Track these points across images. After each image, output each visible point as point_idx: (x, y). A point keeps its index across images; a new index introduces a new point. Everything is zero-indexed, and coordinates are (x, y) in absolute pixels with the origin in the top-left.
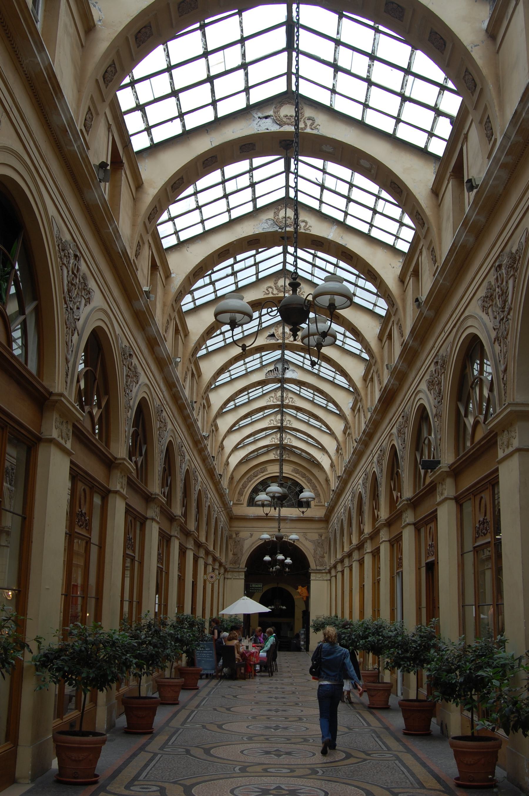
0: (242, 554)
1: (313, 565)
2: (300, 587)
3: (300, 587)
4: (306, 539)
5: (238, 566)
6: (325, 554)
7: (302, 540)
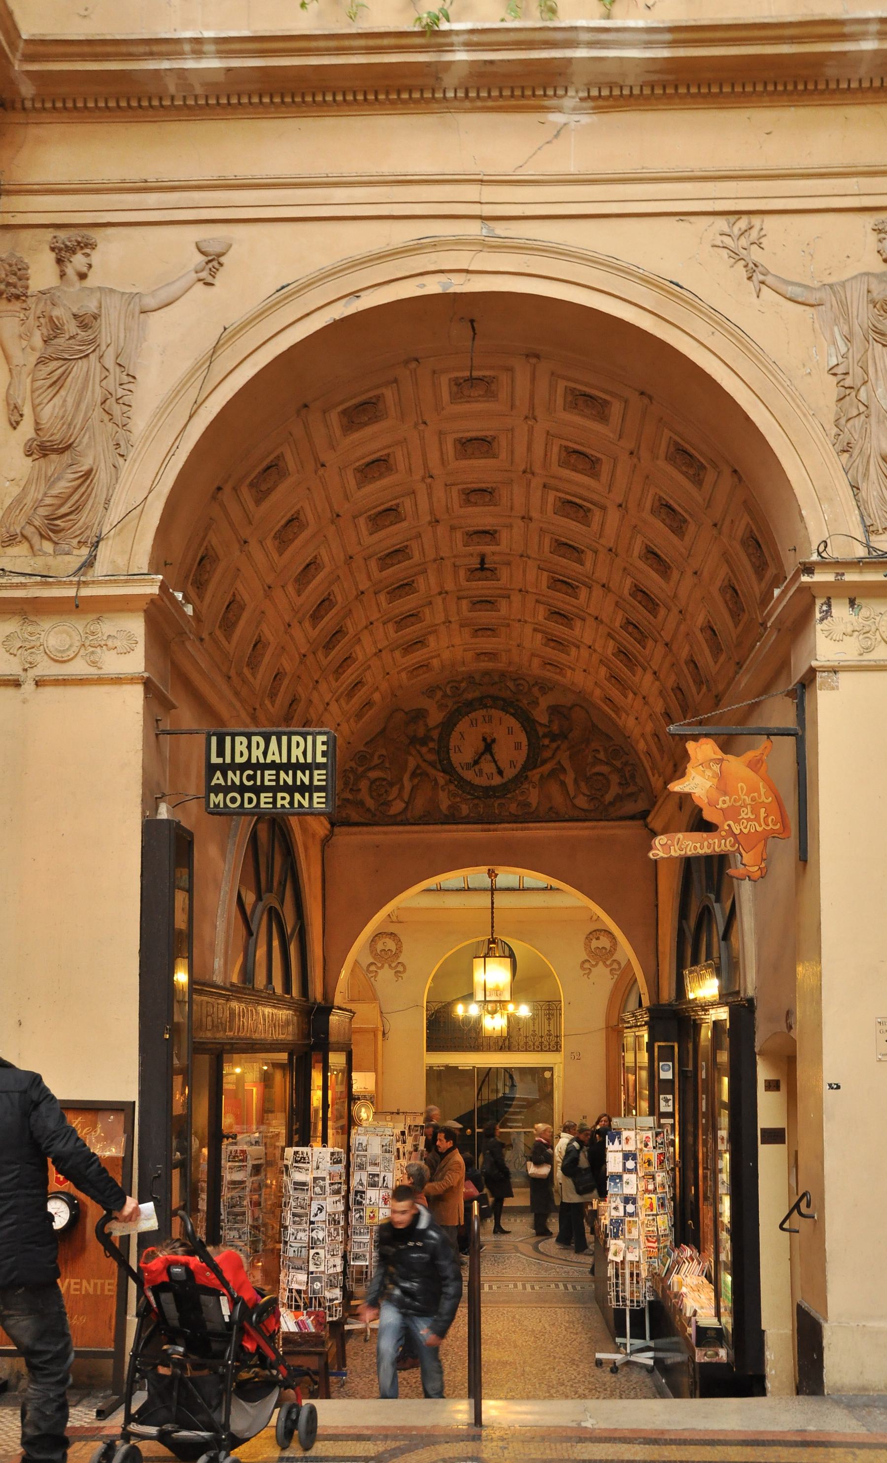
2: (702, 751)
3: (702, 751)
4: (752, 269)
7: (715, 281)
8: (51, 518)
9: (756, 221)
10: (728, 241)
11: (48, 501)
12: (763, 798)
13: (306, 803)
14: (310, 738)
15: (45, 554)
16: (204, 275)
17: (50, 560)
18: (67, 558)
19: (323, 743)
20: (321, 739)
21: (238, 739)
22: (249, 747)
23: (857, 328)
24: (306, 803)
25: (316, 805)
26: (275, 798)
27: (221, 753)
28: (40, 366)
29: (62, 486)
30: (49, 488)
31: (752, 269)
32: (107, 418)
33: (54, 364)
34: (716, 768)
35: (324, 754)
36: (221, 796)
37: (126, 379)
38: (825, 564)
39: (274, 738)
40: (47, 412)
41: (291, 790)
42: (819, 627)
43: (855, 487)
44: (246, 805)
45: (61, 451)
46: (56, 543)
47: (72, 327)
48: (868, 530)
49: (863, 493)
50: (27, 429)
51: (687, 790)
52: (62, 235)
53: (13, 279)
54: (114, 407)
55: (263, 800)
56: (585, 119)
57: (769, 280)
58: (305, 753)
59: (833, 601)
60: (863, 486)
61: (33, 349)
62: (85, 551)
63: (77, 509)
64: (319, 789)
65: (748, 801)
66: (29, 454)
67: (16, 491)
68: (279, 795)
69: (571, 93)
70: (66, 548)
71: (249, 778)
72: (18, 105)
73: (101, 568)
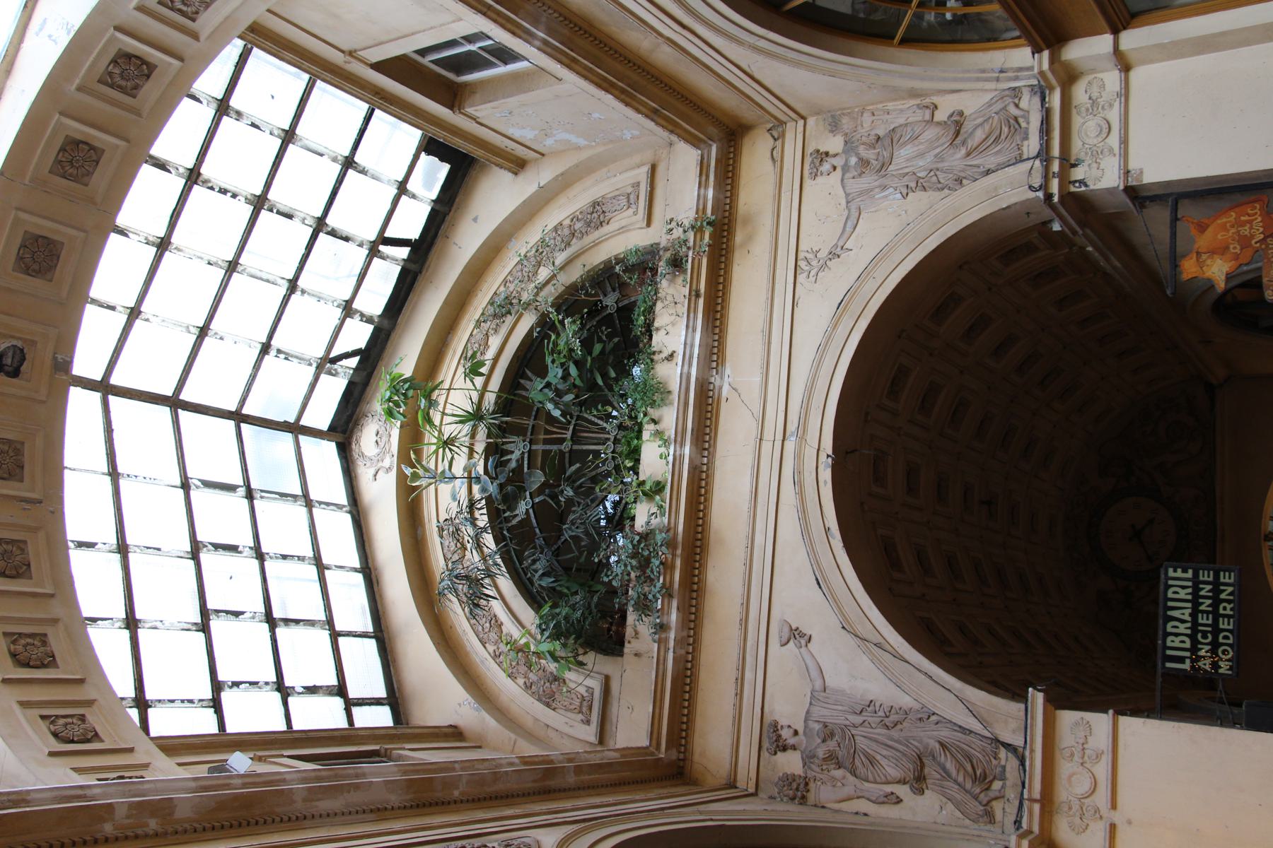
0: (926, 716)
1: (1006, 188)
3: (1189, 268)
4: (833, 255)
5: (1012, 764)
6: (941, 116)
8: (975, 779)
9: (801, 255)
10: (813, 273)
11: (960, 779)
12: (1232, 219)
13: (1230, 589)
14: (1170, 582)
15: (1003, 787)
16: (803, 642)
17: (1008, 783)
18: (1008, 769)
19: (1175, 571)
20: (1171, 573)
21: (1169, 644)
22: (1177, 635)
23: (877, 183)
24: (1230, 589)
25: (1232, 580)
26: (1224, 616)
27: (1181, 660)
28: (858, 772)
29: (950, 765)
30: (949, 776)
31: (833, 255)
32: (899, 726)
33: (857, 762)
34: (1204, 257)
35: (1185, 571)
36: (1221, 664)
37: (872, 708)
38: (1045, 186)
39: (1170, 613)
40: (893, 772)
41: (1216, 602)
42: (1092, 187)
43: (988, 172)
44: (1231, 641)
45: (922, 766)
46: (994, 778)
47: (832, 744)
48: (1019, 160)
49: (992, 167)
50: (903, 791)
51: (1223, 277)
52: (766, 744)
53: (794, 785)
54: (893, 719)
55: (1226, 627)
56: (728, 371)
57: (841, 244)
58: (1183, 587)
59: (1073, 179)
60: (988, 167)
61: (844, 777)
62: (1003, 753)
63: (969, 758)
64: (1217, 576)
65: (1233, 230)
66: (921, 792)
67: (950, 806)
68: (1221, 611)
69: (712, 380)
70: (999, 769)
71: (1205, 637)
72: (681, 764)
73: (1018, 741)
